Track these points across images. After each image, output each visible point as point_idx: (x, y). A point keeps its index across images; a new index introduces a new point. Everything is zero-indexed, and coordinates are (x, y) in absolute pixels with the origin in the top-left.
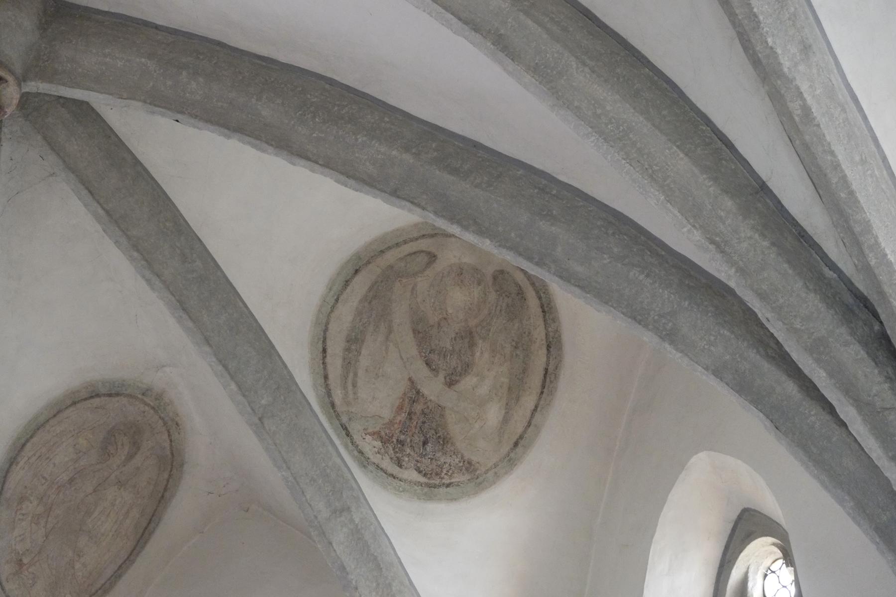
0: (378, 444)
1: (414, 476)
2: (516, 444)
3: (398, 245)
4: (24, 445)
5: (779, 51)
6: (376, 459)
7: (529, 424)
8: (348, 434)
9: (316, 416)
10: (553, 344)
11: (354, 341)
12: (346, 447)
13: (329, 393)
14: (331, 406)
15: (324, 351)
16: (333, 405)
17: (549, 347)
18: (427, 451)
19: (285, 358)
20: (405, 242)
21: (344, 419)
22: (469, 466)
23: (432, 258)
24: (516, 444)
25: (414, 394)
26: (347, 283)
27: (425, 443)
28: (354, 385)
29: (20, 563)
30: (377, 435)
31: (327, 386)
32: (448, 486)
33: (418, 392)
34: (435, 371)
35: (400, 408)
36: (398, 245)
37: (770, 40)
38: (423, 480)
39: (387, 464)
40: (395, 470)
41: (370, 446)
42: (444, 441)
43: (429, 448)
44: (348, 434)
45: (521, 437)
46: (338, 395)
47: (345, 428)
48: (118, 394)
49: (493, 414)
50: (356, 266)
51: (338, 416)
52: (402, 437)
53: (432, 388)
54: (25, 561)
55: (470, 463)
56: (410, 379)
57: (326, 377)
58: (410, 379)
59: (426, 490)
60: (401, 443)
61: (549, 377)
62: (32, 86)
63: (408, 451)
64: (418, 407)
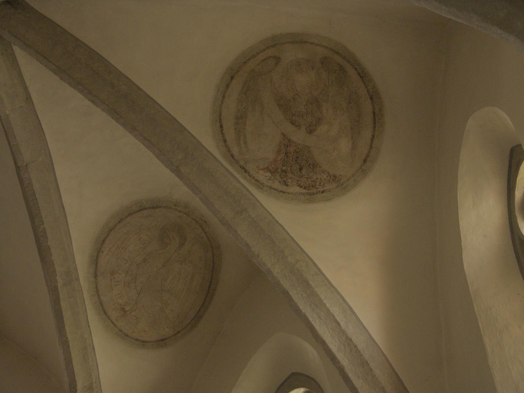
0: (269, 174)
1: (297, 189)
2: (365, 161)
3: (253, 56)
4: (104, 241)
6: (270, 183)
7: (371, 147)
8: (246, 171)
9: (220, 162)
10: (374, 96)
11: (240, 118)
12: (245, 178)
13: (229, 150)
15: (221, 126)
16: (233, 156)
17: (371, 98)
18: (303, 174)
19: (193, 133)
20: (258, 54)
21: (242, 163)
22: (335, 178)
23: (278, 59)
24: (365, 161)
25: (286, 142)
26: (228, 86)
27: (301, 169)
28: (245, 143)
30: (267, 169)
31: (226, 146)
32: (323, 192)
33: (289, 140)
34: (299, 126)
35: (279, 152)
36: (253, 56)
38: (304, 191)
39: (277, 185)
40: (284, 188)
41: (263, 176)
42: (314, 166)
43: (304, 171)
44: (246, 171)
45: (368, 156)
46: (235, 151)
47: (242, 167)
48: (158, 207)
49: (345, 145)
50: (231, 75)
51: (237, 162)
52: (284, 168)
53: (299, 137)
54: (127, 309)
55: (335, 176)
56: (282, 134)
57: (225, 141)
58: (282, 134)
59: (308, 197)
61: (377, 118)
63: (290, 175)
64: (291, 149)
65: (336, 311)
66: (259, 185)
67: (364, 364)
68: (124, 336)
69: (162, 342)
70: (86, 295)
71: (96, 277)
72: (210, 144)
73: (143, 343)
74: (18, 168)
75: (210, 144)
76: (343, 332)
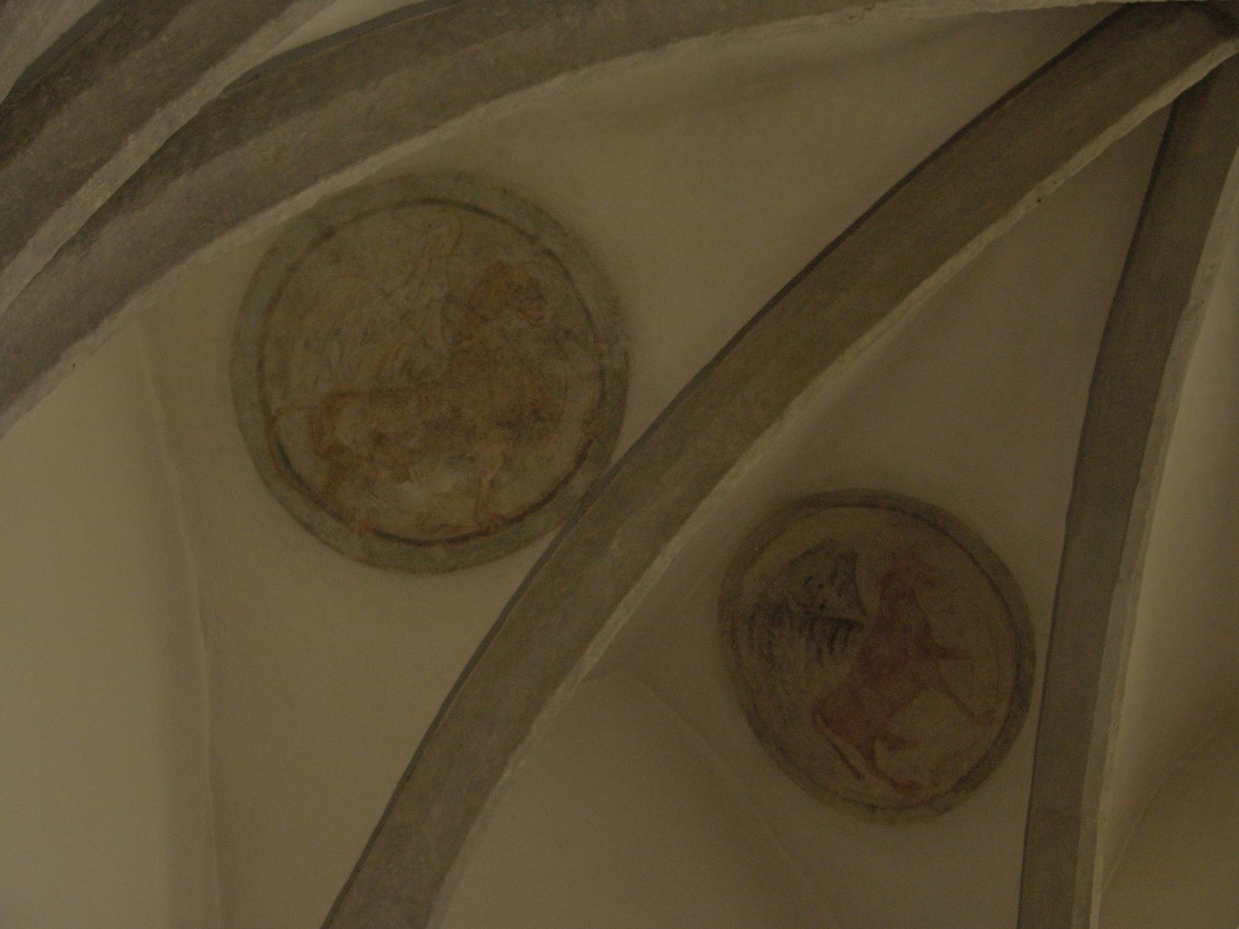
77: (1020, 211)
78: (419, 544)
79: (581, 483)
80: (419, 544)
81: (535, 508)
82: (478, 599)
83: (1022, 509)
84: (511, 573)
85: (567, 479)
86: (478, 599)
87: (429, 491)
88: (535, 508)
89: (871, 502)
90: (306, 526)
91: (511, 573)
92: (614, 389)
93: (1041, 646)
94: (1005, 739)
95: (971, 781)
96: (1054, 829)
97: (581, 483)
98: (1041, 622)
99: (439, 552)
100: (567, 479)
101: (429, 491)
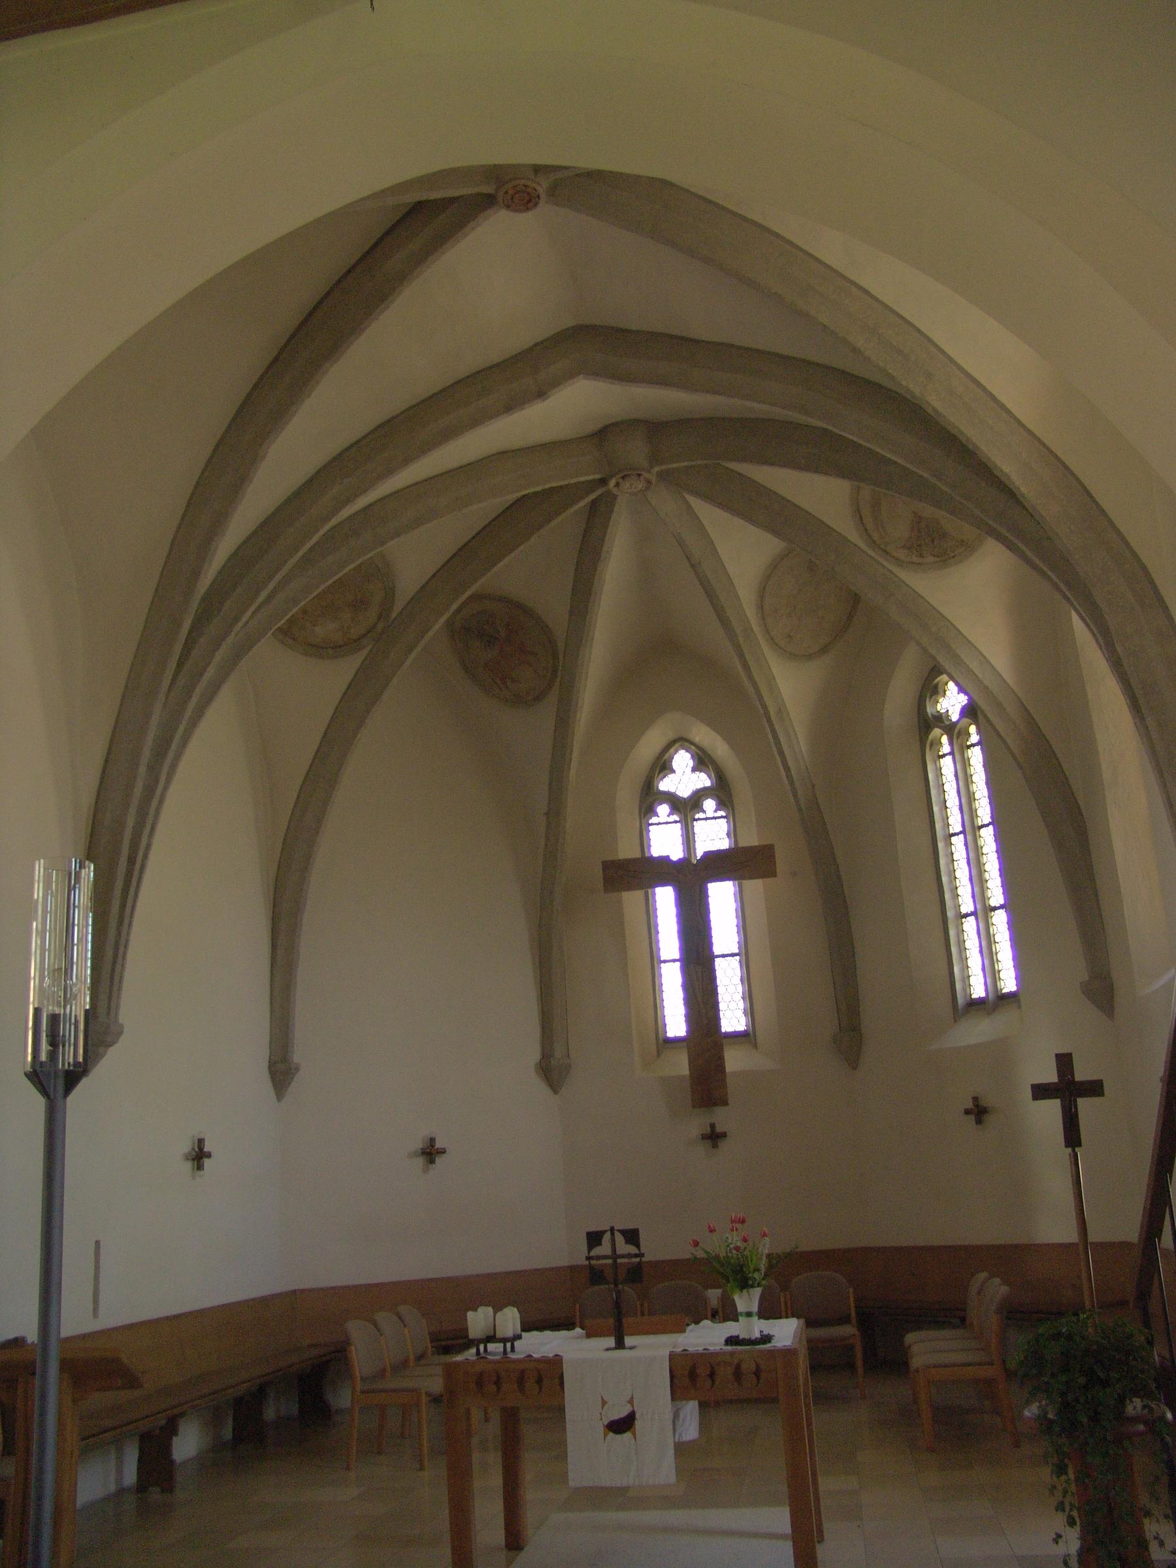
1: (931, 559)
5: (911, 386)
9: (864, 552)
14: (873, 543)
22: (962, 542)
29: (790, 636)
30: (904, 547)
37: (904, 383)
39: (915, 559)
40: (920, 560)
41: (902, 554)
42: (944, 536)
43: (936, 542)
46: (876, 536)
60: (920, 545)
62: (656, 469)
65: (974, 666)
66: (900, 563)
67: (999, 705)
68: (793, 656)
69: (824, 650)
70: (760, 637)
71: (764, 619)
72: (854, 536)
73: (810, 657)
74: (693, 566)
75: (854, 536)
76: (982, 682)
77: (532, 539)
78: (323, 648)
79: (380, 626)
80: (323, 648)
81: (364, 636)
82: (344, 670)
83: (553, 606)
84: (357, 660)
85: (375, 626)
86: (344, 670)
87: (325, 630)
88: (364, 636)
89: (501, 599)
90: (283, 642)
91: (357, 660)
92: (390, 594)
93: (561, 658)
94: (550, 686)
95: (538, 698)
96: (564, 722)
97: (380, 626)
98: (561, 645)
99: (330, 651)
100: (375, 626)
101: (325, 630)
